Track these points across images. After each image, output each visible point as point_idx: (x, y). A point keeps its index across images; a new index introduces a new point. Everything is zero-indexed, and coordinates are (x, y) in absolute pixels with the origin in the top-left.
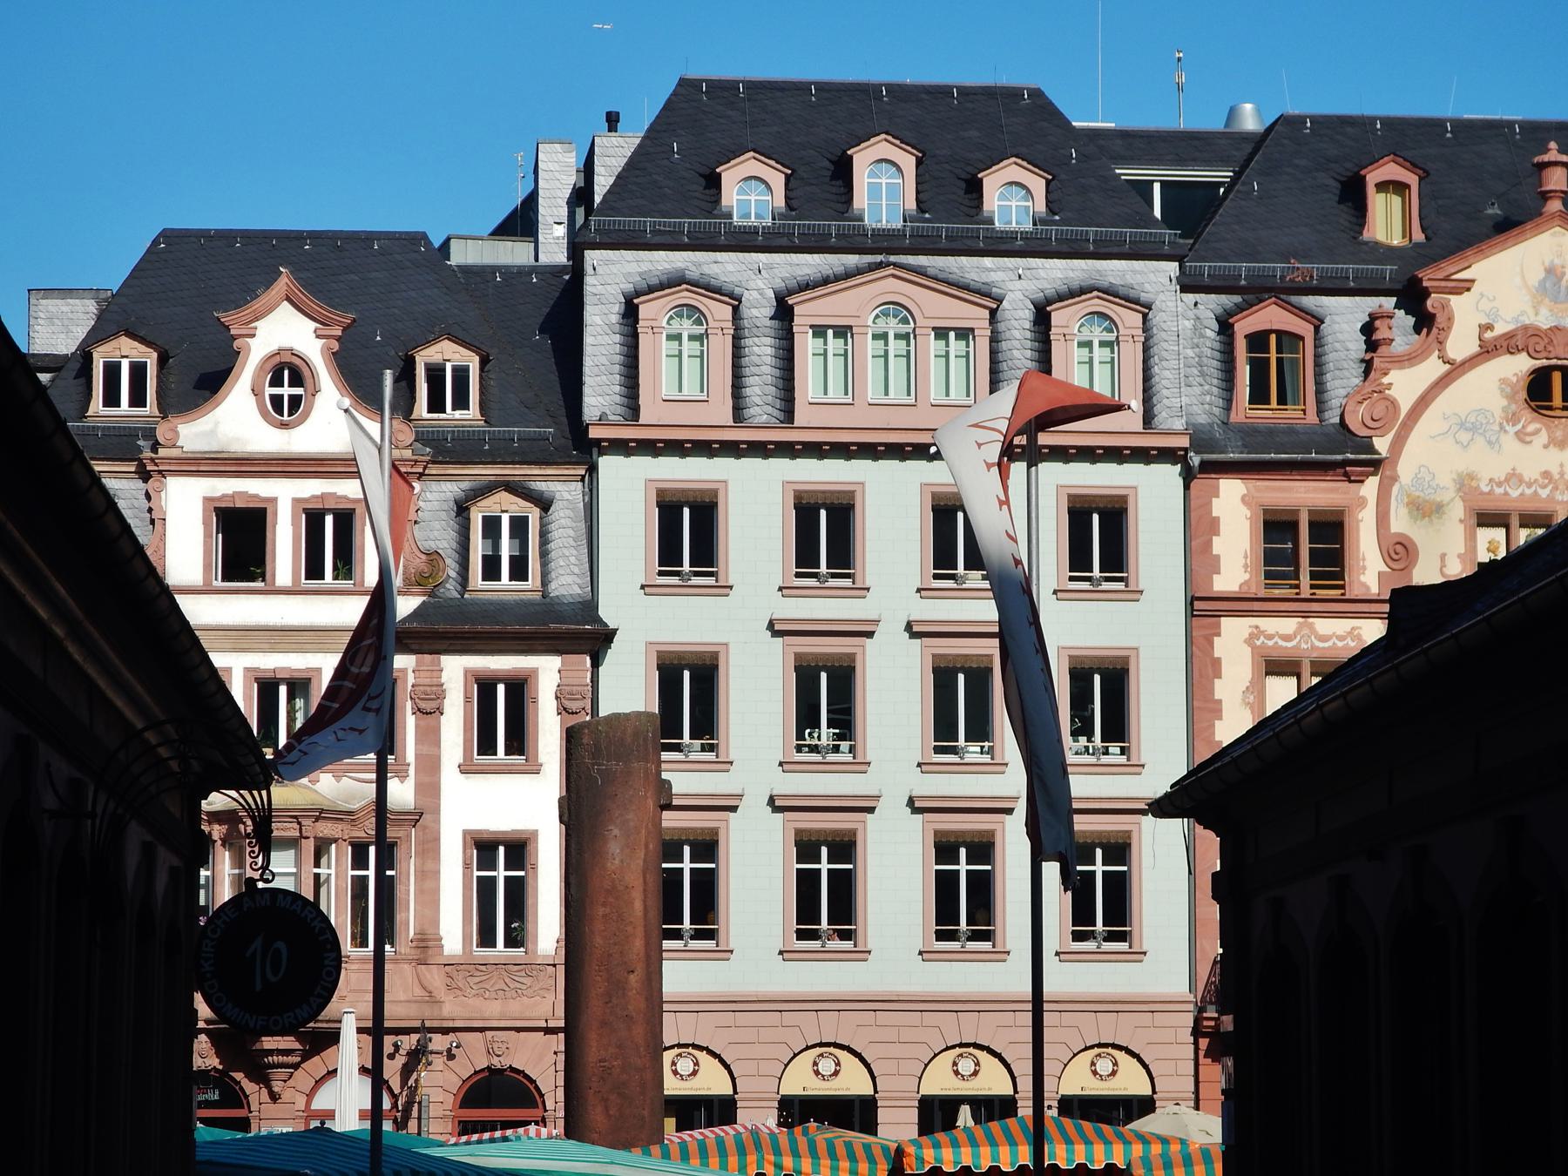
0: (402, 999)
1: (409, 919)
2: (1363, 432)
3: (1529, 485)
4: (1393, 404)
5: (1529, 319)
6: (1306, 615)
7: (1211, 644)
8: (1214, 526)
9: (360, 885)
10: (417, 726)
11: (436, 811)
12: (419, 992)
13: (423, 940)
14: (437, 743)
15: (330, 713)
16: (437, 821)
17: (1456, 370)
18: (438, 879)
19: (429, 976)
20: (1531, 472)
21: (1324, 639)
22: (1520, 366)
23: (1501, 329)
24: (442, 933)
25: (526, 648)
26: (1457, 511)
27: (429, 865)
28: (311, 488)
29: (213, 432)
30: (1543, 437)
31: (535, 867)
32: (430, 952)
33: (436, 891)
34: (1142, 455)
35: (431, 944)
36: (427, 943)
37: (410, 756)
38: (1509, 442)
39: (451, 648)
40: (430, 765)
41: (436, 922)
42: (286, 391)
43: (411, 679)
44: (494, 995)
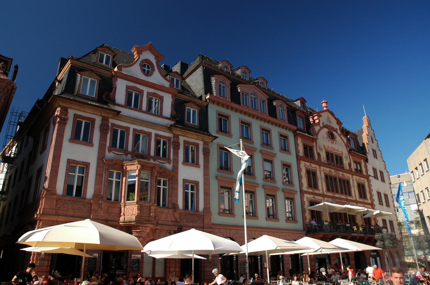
0: (170, 220)
2: (313, 135)
3: (330, 148)
4: (316, 131)
5: (327, 123)
6: (310, 162)
7: (300, 165)
8: (298, 144)
10: (173, 152)
12: (174, 219)
14: (178, 156)
15: (164, 139)
16: (178, 176)
17: (321, 128)
19: (176, 215)
20: (330, 147)
21: (313, 167)
22: (325, 130)
23: (325, 124)
24: (178, 204)
25: (197, 138)
26: (324, 151)
28: (152, 90)
29: (130, 71)
30: (330, 142)
33: (177, 193)
34: (290, 130)
36: (175, 207)
37: (172, 158)
38: (328, 142)
39: (182, 135)
40: (176, 161)
41: (177, 201)
42: (146, 69)
43: (172, 140)
44: (190, 222)
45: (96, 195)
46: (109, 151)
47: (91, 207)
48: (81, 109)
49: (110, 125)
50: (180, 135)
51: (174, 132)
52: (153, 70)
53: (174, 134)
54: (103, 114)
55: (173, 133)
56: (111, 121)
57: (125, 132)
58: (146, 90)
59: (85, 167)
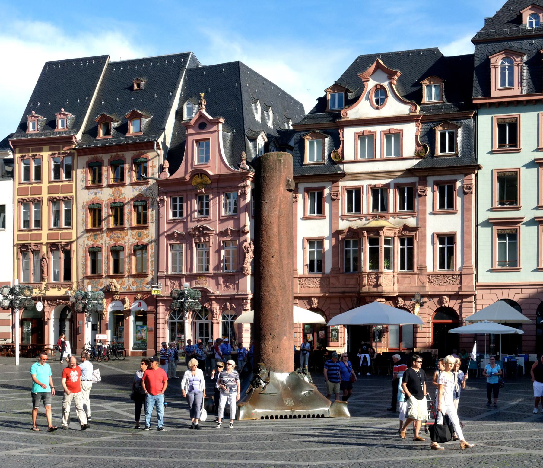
0: (414, 286)
1: (416, 260)
9: (402, 250)
11: (425, 227)
12: (419, 283)
13: (421, 267)
16: (425, 230)
18: (425, 248)
27: (423, 244)
28: (386, 128)
29: (357, 112)
31: (456, 244)
32: (423, 271)
33: (425, 252)
35: (423, 268)
36: (422, 268)
41: (425, 262)
45: (333, 269)
46: (343, 217)
47: (329, 281)
48: (309, 181)
49: (340, 189)
50: (428, 176)
51: (418, 175)
52: (386, 96)
53: (420, 177)
54: (331, 180)
55: (417, 176)
56: (342, 184)
57: (358, 191)
58: (379, 129)
59: (320, 242)
